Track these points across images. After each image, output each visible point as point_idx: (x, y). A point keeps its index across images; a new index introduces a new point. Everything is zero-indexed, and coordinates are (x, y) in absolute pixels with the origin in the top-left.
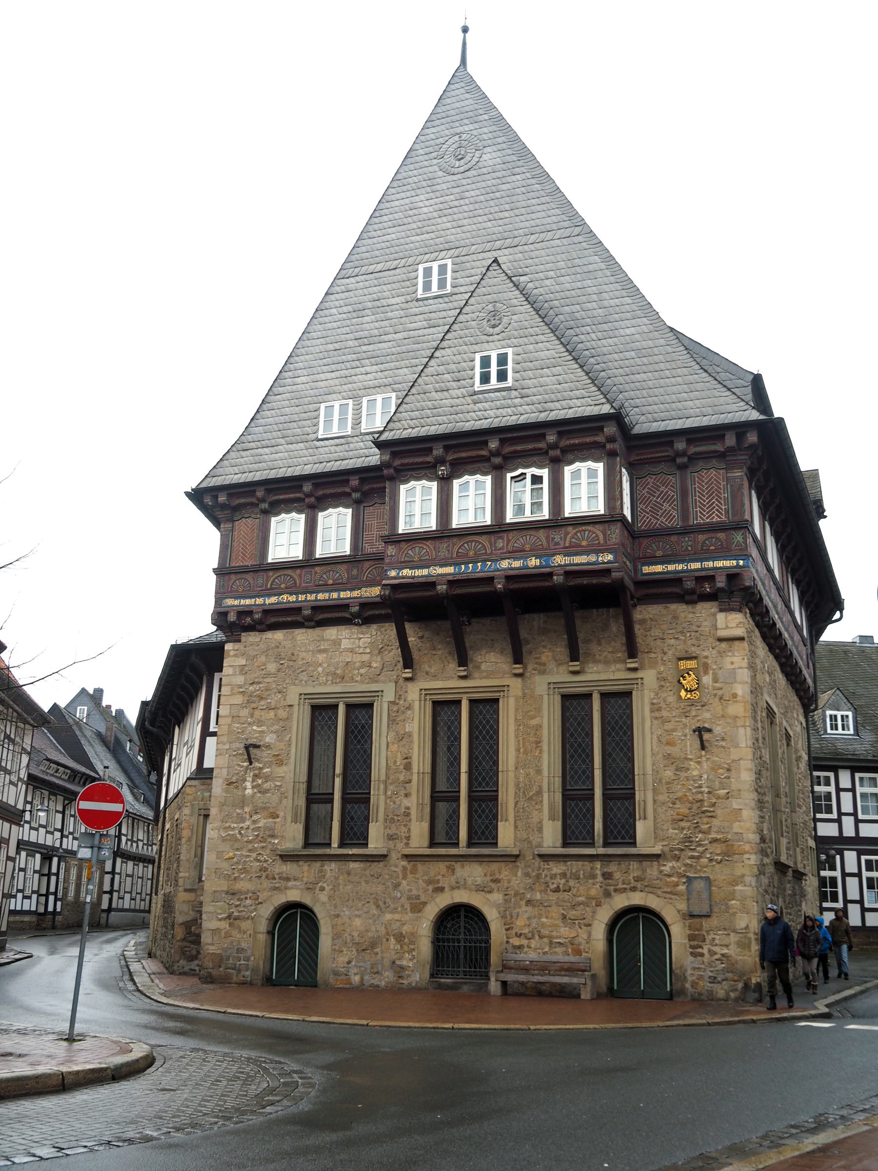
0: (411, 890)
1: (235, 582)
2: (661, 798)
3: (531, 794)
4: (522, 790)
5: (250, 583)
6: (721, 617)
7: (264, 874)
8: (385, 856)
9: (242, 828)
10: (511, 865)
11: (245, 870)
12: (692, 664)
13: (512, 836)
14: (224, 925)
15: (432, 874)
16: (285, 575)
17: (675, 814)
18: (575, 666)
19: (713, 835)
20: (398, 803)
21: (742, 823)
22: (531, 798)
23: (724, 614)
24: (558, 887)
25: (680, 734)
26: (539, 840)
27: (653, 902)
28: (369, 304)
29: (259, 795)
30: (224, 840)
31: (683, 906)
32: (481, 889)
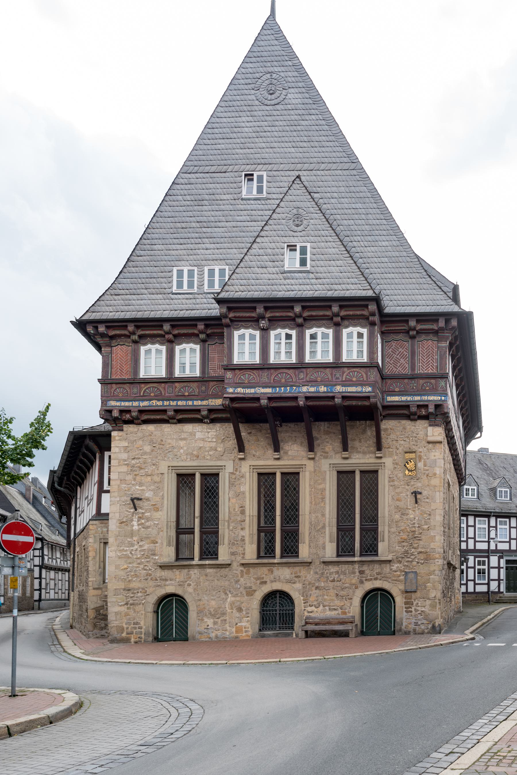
0: (246, 584)
1: (116, 389)
3: (319, 528)
5: (127, 391)
7: (150, 578)
8: (230, 565)
9: (132, 550)
11: (136, 576)
14: (124, 609)
16: (153, 387)
20: (237, 534)
22: (319, 530)
29: (143, 529)
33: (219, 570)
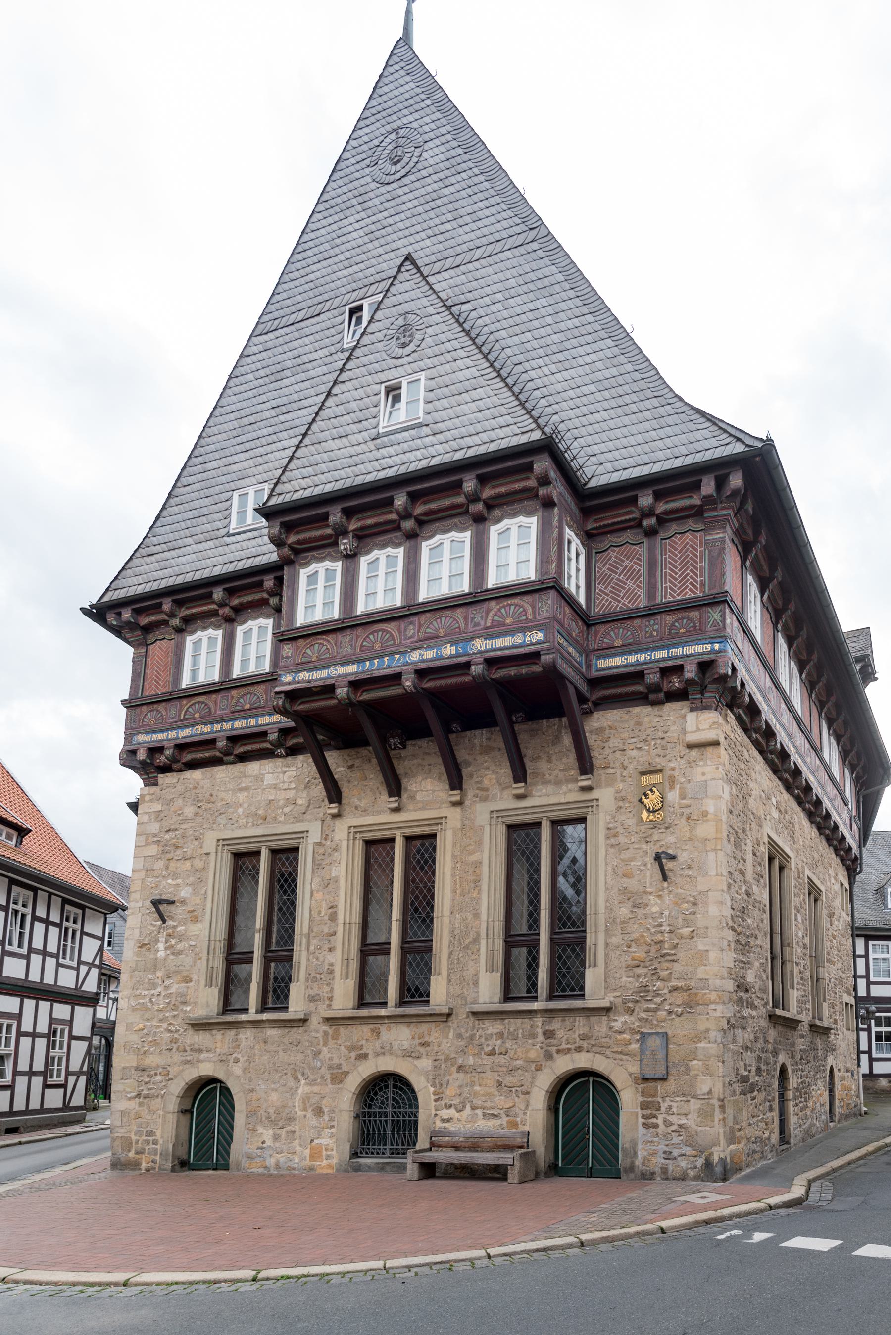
0: (331, 1059)
2: (615, 940)
3: (467, 942)
4: (457, 938)
6: (691, 717)
7: (175, 1046)
9: (153, 995)
10: (442, 1025)
11: (155, 1043)
12: (656, 778)
13: (444, 991)
14: (133, 1105)
15: (355, 1039)
17: (629, 959)
18: (520, 788)
19: (674, 983)
20: (321, 959)
21: (707, 968)
22: (467, 947)
23: (695, 713)
24: (494, 1049)
25: (639, 863)
26: (474, 995)
27: (600, 1064)
28: (289, 364)
29: (172, 957)
30: (134, 1009)
31: (634, 1068)
32: (409, 1054)
33: (287, 1030)
